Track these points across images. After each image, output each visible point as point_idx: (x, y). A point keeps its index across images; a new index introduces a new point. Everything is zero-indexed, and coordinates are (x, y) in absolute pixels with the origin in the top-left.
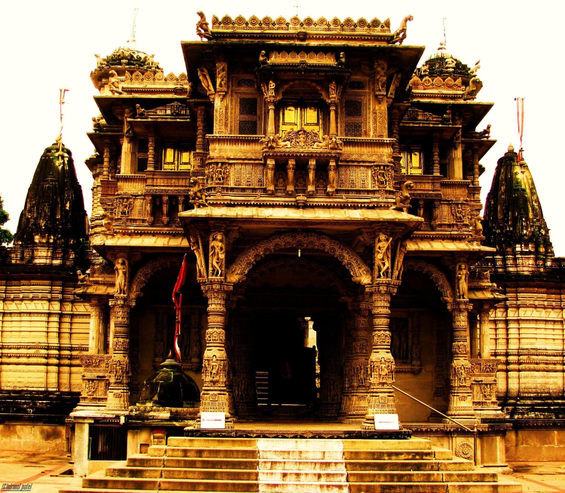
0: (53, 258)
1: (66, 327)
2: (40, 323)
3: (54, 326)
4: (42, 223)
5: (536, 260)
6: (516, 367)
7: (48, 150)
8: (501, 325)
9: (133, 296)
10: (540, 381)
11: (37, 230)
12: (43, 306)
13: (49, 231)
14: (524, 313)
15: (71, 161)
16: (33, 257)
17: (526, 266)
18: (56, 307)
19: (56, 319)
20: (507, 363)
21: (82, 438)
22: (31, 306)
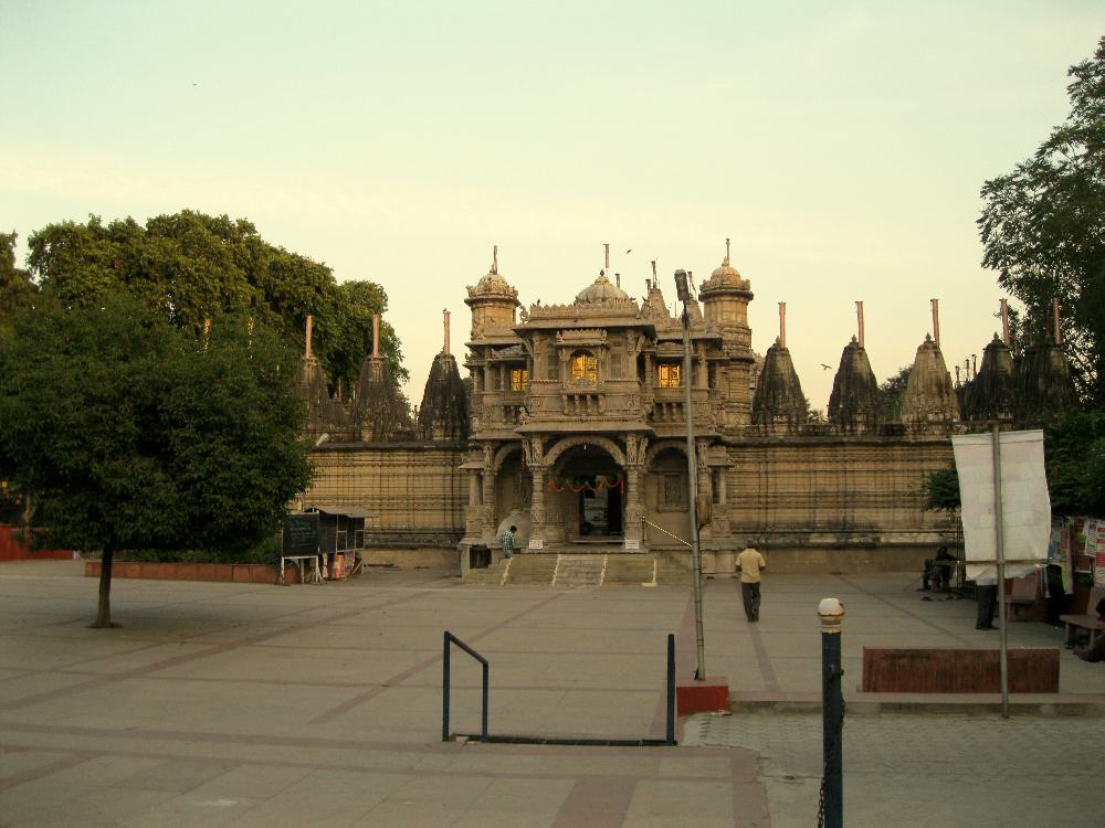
0: (445, 436)
1: (456, 483)
2: (438, 480)
3: (448, 483)
4: (437, 412)
5: (789, 427)
6: (773, 505)
7: (437, 357)
8: (763, 475)
9: (496, 469)
10: (791, 515)
11: (434, 417)
12: (441, 470)
13: (442, 417)
14: (779, 467)
15: (455, 364)
16: (432, 436)
17: (781, 432)
18: (449, 469)
19: (449, 478)
20: (767, 503)
21: (466, 559)
22: (428, 470)
